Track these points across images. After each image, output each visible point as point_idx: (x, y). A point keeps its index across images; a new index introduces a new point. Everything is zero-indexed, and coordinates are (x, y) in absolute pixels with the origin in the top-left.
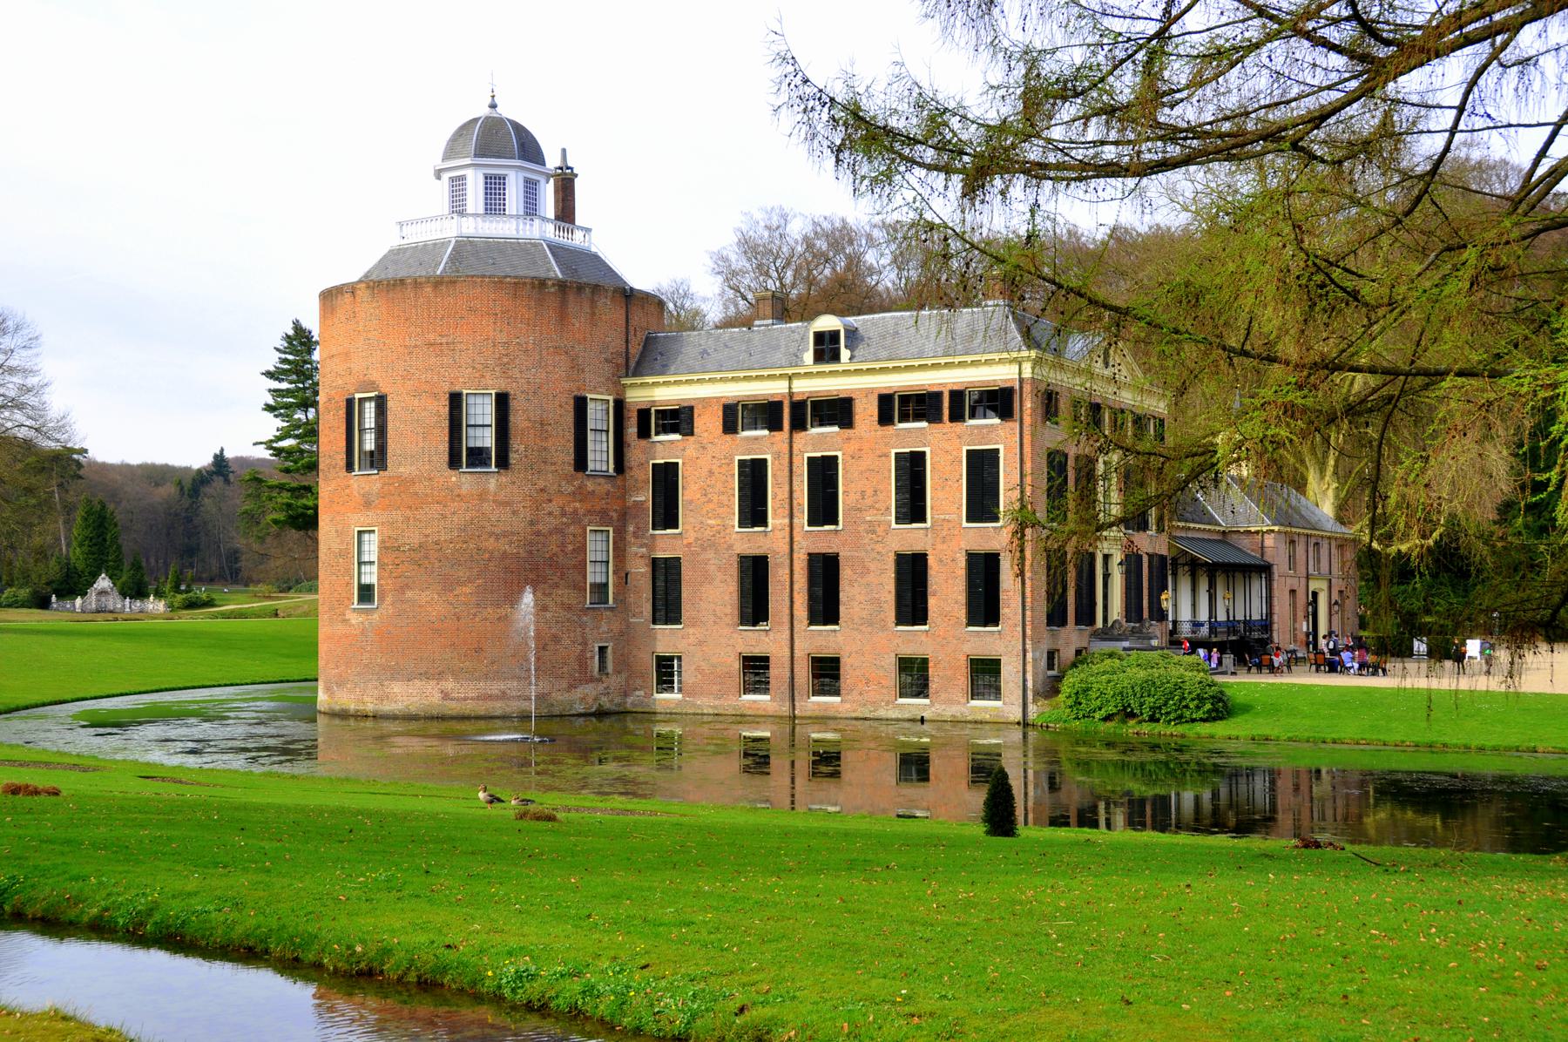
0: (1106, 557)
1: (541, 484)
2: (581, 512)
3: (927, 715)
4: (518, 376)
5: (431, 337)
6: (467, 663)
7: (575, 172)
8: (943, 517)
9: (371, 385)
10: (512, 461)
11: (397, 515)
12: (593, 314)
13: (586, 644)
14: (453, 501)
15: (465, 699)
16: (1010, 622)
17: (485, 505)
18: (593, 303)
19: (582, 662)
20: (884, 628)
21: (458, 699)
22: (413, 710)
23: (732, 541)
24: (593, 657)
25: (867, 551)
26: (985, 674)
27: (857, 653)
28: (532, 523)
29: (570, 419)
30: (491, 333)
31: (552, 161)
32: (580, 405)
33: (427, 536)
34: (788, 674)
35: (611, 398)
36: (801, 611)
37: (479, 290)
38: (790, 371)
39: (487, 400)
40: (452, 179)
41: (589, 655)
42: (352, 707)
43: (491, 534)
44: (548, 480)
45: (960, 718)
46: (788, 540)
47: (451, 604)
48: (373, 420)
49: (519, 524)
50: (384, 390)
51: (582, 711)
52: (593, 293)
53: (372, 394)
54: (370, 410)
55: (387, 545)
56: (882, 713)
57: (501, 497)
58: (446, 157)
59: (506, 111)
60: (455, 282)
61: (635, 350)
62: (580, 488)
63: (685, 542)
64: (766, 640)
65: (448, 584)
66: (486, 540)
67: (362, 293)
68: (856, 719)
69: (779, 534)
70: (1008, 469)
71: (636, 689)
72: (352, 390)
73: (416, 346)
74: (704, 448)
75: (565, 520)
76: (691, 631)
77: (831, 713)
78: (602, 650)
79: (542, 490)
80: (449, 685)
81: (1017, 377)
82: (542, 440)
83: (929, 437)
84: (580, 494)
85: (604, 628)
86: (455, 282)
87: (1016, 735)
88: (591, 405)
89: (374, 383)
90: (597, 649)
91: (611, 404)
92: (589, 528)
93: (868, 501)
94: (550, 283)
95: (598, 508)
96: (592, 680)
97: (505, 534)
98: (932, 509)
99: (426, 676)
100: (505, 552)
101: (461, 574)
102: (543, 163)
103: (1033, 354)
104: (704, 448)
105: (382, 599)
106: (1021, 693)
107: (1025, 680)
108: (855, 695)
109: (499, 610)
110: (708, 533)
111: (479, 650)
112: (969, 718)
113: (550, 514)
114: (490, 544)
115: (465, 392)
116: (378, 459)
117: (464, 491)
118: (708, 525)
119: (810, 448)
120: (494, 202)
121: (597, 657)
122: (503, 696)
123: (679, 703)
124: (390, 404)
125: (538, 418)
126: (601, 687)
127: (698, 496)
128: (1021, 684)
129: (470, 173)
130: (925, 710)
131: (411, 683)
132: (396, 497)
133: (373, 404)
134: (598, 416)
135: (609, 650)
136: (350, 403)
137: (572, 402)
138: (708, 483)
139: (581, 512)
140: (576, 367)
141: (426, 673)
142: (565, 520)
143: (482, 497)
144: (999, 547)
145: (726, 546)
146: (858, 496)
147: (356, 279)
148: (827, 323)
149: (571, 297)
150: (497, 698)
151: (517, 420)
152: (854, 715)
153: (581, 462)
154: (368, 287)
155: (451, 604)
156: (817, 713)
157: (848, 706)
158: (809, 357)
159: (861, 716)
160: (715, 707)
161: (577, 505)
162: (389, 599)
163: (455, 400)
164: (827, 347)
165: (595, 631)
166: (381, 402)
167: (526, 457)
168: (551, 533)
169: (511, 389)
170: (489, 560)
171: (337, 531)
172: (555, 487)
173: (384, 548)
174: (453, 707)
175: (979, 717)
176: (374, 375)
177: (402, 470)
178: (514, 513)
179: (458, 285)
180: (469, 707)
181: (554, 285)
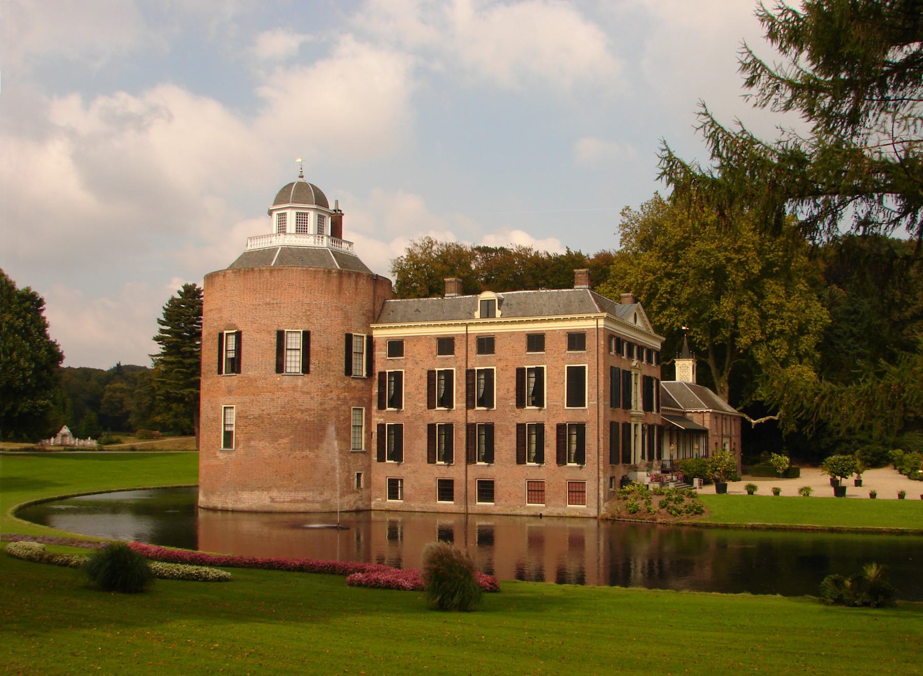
0: (636, 426)
1: (327, 382)
2: (348, 398)
3: (544, 513)
4: (315, 322)
5: (268, 300)
6: (285, 482)
7: (342, 212)
8: (553, 403)
10: (311, 369)
11: (247, 399)
12: (357, 289)
13: (350, 472)
14: (278, 391)
15: (284, 502)
16: (591, 462)
17: (296, 393)
18: (356, 283)
19: (348, 482)
21: (280, 502)
22: (254, 508)
23: (433, 415)
24: (354, 479)
25: (510, 422)
26: (576, 492)
27: (503, 478)
28: (321, 404)
29: (343, 346)
30: (301, 298)
31: (332, 207)
32: (349, 338)
33: (263, 410)
34: (464, 490)
35: (365, 335)
37: (295, 274)
38: (467, 322)
39: (298, 335)
40: (278, 214)
41: (351, 478)
42: (220, 506)
43: (300, 410)
44: (330, 380)
45: (562, 515)
46: (465, 415)
47: (276, 449)
48: (234, 345)
49: (314, 405)
50: (240, 329)
51: (348, 509)
52: (357, 277)
53: (234, 331)
54: (232, 341)
55: (241, 415)
56: (518, 512)
57: (305, 390)
58: (276, 203)
59: (307, 179)
60: (282, 270)
61: (378, 309)
62: (348, 385)
63: (406, 415)
65: (275, 438)
66: (296, 413)
67: (230, 275)
69: (460, 412)
70: (591, 378)
71: (377, 497)
72: (222, 329)
73: (259, 305)
74: (417, 363)
75: (339, 402)
76: (408, 465)
77: (489, 512)
78: (359, 475)
79: (327, 386)
80: (275, 494)
81: (596, 327)
82: (328, 358)
83: (546, 359)
84: (348, 388)
85: (360, 463)
86: (282, 270)
87: (594, 523)
88: (354, 339)
89: (235, 325)
90: (356, 475)
91: (365, 339)
92: (352, 407)
94: (334, 271)
95: (357, 396)
96: (353, 492)
97: (307, 410)
98: (547, 398)
99: (261, 489)
100: (306, 420)
101: (281, 432)
102: (328, 208)
103: (605, 315)
104: (417, 363)
105: (237, 445)
106: (596, 501)
107: (599, 494)
108: (502, 502)
109: (303, 453)
110: (419, 411)
111: (291, 475)
112: (567, 515)
113: (331, 399)
114: (299, 415)
115: (286, 330)
116: (235, 365)
117: (284, 385)
118: (419, 407)
119: (478, 364)
120: (301, 228)
121: (356, 479)
122: (304, 500)
123: (402, 505)
125: (325, 346)
126: (357, 496)
127: (414, 390)
128: (597, 496)
129: (288, 212)
130: (542, 510)
131: (253, 493)
132: (246, 389)
133: (234, 337)
134: (359, 345)
135: (362, 475)
136: (221, 335)
137: (344, 337)
138: (419, 383)
139: (348, 398)
140: (346, 317)
141: (262, 487)
142: (339, 402)
143: (294, 388)
144: (585, 421)
145: (429, 418)
146: (505, 391)
148: (488, 295)
149: (345, 280)
150: (302, 501)
151: (313, 346)
152: (502, 513)
153: (348, 371)
154: (233, 272)
155: (276, 449)
156: (481, 512)
157: (498, 508)
158: (477, 314)
159: (506, 513)
160: (422, 508)
161: (346, 394)
162: (241, 446)
163: (281, 335)
164: (488, 310)
165: (355, 465)
166: (238, 335)
167: (319, 367)
168: (332, 409)
169: (311, 328)
170: (298, 425)
171: (212, 407)
172: (334, 384)
173: (239, 417)
174: (278, 507)
175: (573, 514)
176: (235, 321)
177: (249, 373)
178: (312, 398)
179: (284, 272)
180: (286, 507)
181: (335, 273)
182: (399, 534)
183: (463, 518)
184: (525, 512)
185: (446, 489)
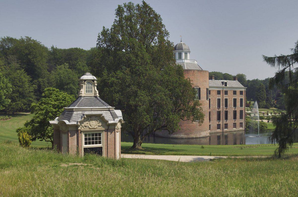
9: (198, 86)
20: (232, 120)
22: (204, 136)
36: (224, 118)
50: (200, 87)
56: (232, 130)
64: (221, 123)
68: (230, 131)
80: (207, 132)
93: (231, 104)
124: (201, 89)
147: (235, 75)
158: (224, 85)
176: (198, 85)
182: (224, 138)
183: (222, 133)
184: (233, 130)
185: (219, 127)
